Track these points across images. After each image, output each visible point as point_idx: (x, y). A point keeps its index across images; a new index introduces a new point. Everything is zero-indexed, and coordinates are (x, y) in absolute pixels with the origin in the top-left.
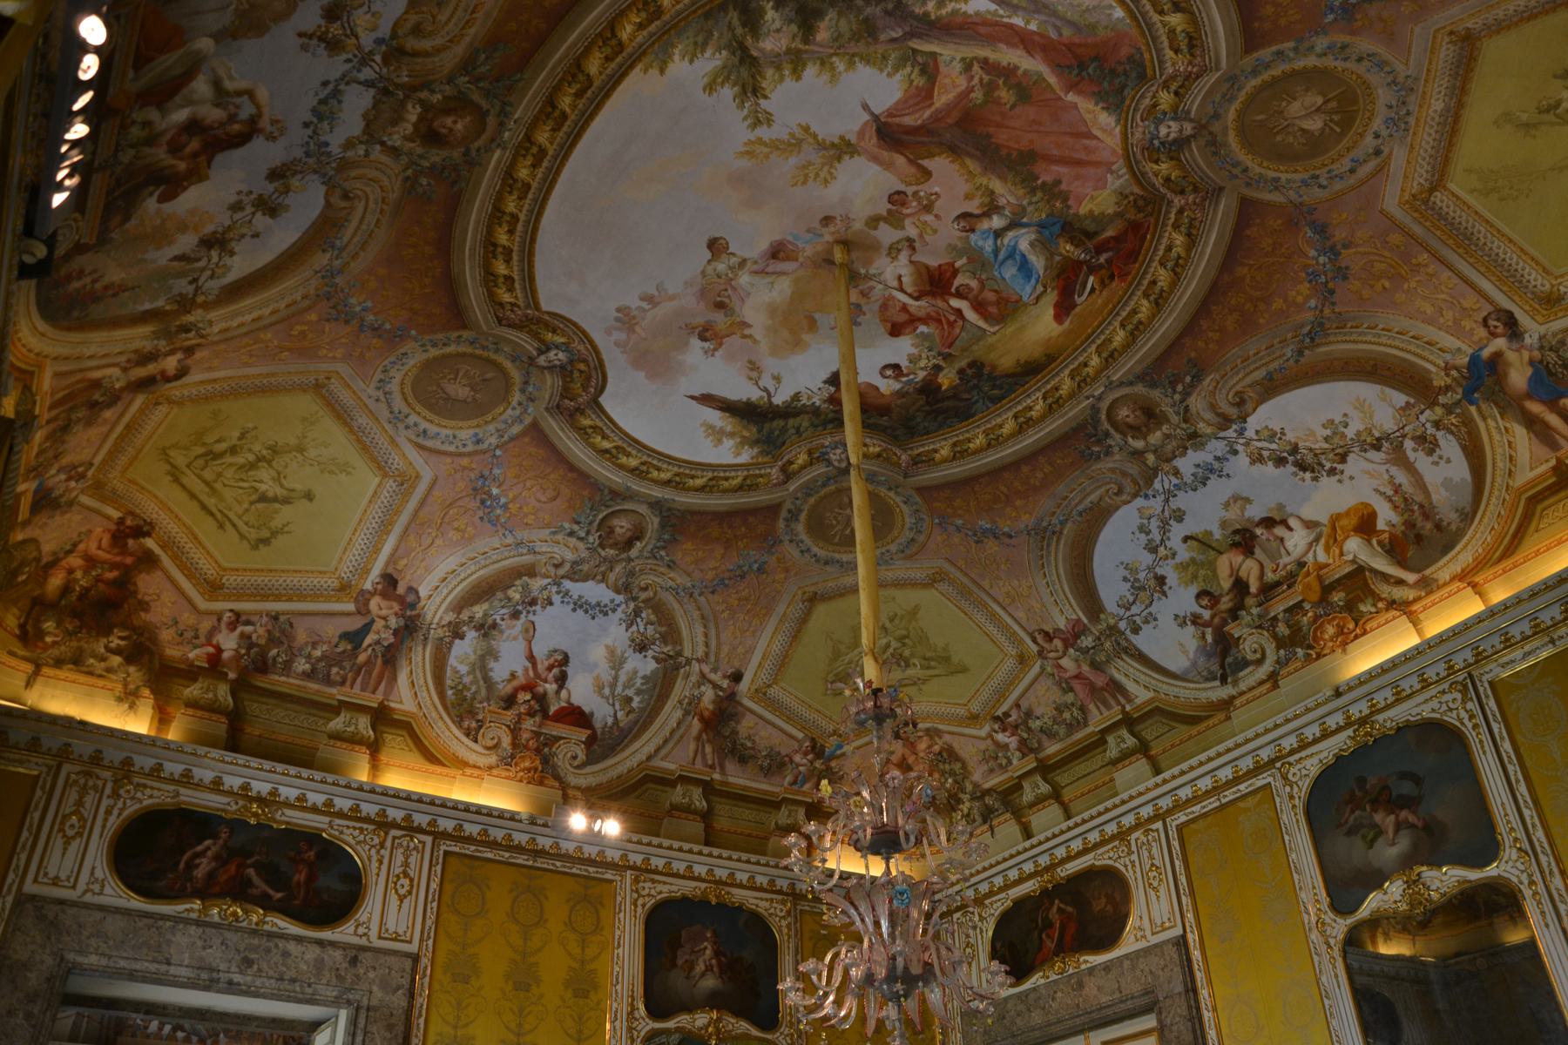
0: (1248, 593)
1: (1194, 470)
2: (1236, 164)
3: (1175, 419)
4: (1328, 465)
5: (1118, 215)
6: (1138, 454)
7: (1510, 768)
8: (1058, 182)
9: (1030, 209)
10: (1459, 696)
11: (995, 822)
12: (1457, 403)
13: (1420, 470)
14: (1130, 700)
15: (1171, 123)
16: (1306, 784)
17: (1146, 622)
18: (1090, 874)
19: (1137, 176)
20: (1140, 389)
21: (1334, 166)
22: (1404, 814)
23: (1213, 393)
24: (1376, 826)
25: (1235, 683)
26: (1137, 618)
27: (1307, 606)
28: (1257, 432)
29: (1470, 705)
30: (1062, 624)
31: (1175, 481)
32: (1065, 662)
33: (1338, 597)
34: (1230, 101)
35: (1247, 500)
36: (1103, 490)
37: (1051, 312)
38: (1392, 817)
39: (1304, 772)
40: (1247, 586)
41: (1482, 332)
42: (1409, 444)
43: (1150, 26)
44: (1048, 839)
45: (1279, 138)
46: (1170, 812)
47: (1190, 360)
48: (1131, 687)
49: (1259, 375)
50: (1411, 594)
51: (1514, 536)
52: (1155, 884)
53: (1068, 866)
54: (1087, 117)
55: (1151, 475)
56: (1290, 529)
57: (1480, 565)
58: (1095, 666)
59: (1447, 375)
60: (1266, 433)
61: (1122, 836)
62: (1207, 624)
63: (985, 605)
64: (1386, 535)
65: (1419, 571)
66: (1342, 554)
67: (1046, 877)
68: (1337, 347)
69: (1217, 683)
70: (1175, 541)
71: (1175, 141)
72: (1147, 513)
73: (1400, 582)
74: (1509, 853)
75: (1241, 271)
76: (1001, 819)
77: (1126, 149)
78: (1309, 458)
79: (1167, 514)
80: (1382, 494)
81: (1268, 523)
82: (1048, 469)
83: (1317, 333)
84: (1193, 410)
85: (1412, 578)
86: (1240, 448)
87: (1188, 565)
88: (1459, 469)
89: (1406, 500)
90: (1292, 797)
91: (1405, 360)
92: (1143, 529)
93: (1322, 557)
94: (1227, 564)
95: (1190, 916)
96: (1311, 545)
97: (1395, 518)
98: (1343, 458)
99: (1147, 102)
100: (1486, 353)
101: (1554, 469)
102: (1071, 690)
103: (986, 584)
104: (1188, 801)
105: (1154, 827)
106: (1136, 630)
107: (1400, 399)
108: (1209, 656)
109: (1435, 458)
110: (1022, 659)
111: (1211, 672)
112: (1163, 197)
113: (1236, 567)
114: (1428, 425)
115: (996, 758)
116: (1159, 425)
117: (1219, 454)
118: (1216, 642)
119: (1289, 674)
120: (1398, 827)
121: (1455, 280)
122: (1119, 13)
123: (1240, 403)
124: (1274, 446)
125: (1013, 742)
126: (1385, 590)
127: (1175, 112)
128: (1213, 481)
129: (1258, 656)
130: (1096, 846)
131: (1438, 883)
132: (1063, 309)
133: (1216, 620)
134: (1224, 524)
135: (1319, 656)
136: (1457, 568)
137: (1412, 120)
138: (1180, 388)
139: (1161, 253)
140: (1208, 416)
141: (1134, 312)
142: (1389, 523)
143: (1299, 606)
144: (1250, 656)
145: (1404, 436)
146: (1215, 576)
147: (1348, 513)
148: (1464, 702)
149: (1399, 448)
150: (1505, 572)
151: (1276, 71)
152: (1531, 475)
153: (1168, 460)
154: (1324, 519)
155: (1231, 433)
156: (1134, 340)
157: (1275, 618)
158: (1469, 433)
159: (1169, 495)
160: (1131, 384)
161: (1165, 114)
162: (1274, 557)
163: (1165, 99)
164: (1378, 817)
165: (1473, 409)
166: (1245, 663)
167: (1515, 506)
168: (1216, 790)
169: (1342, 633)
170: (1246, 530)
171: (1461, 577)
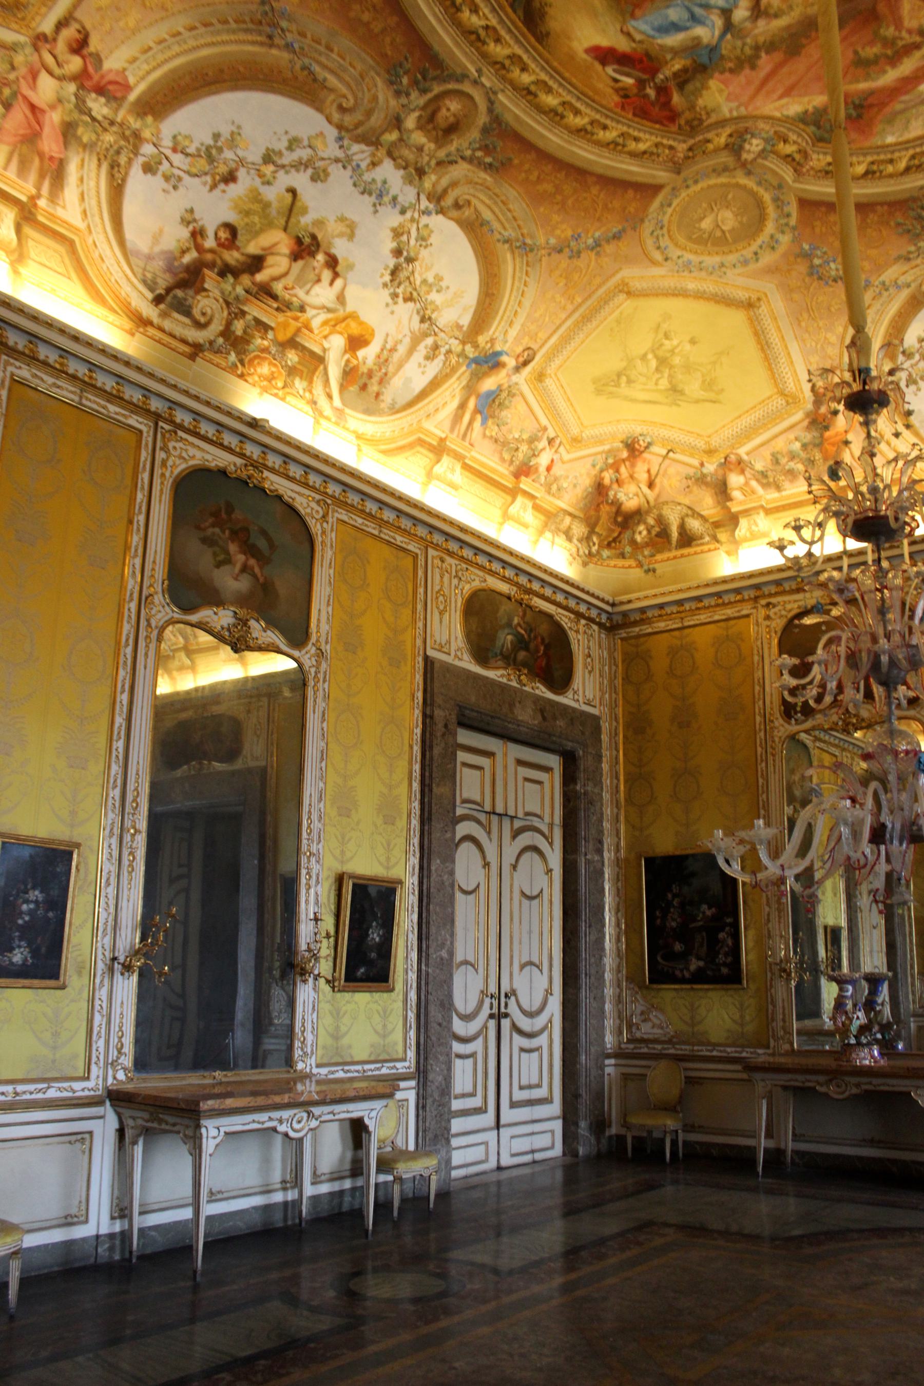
0: (252, 274)
2: (696, 182)
3: (441, 154)
4: (400, 291)
5: (692, 107)
6: (397, 122)
8: (753, 67)
9: (739, 43)
12: (466, 357)
15: (760, 148)
17: (167, 178)
19: (722, 123)
20: (483, 118)
21: (666, 237)
22: (252, 562)
23: (470, 182)
24: (227, 552)
26: (165, 165)
27: (270, 335)
28: (427, 226)
31: (363, 165)
33: (292, 357)
34: (759, 184)
35: (351, 236)
36: (344, 90)
37: (604, 42)
39: (184, 454)
41: (519, 349)
42: (430, 341)
43: (865, 155)
45: (704, 205)
47: (510, 160)
48: (70, 192)
49: (487, 215)
50: (328, 411)
54: (806, 99)
55: (371, 140)
56: (332, 283)
57: (371, 441)
58: (68, 131)
60: (425, 233)
62: (199, 248)
64: (355, 362)
68: (509, 265)
69: (150, 296)
70: (285, 180)
71: (741, 148)
72: (318, 143)
73: (330, 396)
74: (311, 648)
75: (595, 190)
77: (756, 118)
78: (402, 275)
79: (319, 164)
80: (386, 342)
81: (332, 262)
82: (377, 27)
83: (524, 248)
84: (452, 168)
85: (337, 402)
86: (408, 215)
87: (260, 201)
88: (420, 382)
89: (386, 360)
91: (497, 313)
92: (293, 143)
93: (316, 323)
94: (277, 241)
96: (323, 307)
97: (370, 362)
98: (409, 299)
99: (793, 137)
100: (504, 358)
101: (442, 440)
104: (45, 364)
106: (148, 169)
107: (466, 321)
108: (170, 269)
109: (423, 362)
111: (155, 283)
112: (693, 137)
113: (274, 250)
116: (436, 141)
117: (400, 199)
119: (210, 362)
120: (245, 569)
121: (558, 322)
122: (890, 140)
123: (457, 206)
124: (412, 242)
127: (772, 152)
128: (368, 200)
129: (202, 320)
132: (604, 55)
133: (209, 257)
134: (319, 223)
135: (241, 376)
137: (686, 273)
138: (479, 154)
139: (636, 134)
140: (444, 182)
141: (577, 112)
142: (365, 359)
143: (266, 328)
144: (196, 312)
146: (256, 234)
147: (361, 323)
149: (425, 335)
151: (771, 210)
153: (390, 154)
154: (350, 308)
155: (424, 203)
156: (545, 113)
157: (243, 313)
159: (345, 162)
160: (490, 111)
161: (773, 146)
162: (300, 281)
163: (789, 149)
164: (233, 548)
165: (464, 368)
166: (187, 312)
167: (412, 433)
169: (270, 381)
171: (359, 437)
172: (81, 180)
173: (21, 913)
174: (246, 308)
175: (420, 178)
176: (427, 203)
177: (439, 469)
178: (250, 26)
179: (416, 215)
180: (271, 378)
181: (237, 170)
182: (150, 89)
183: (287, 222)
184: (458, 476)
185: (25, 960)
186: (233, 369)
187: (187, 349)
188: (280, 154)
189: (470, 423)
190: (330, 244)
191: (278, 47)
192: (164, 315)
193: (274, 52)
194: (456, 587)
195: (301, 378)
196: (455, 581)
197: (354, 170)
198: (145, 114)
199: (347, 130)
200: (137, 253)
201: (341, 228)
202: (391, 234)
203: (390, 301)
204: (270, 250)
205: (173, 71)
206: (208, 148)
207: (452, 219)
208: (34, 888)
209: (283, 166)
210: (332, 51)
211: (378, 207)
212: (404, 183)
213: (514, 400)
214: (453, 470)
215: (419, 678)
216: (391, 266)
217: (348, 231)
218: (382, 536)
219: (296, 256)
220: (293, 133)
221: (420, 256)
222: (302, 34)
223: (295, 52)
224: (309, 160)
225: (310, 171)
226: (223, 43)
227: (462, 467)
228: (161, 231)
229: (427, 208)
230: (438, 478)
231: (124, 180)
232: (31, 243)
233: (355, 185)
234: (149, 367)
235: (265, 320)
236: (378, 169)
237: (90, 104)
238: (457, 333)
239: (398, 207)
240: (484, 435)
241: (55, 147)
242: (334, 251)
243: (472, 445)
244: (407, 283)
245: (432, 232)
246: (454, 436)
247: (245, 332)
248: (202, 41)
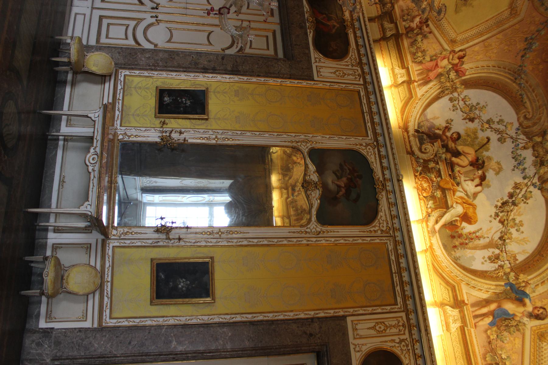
0: (453, 156)
1: (523, 156)
4: (501, 214)
7: (351, 239)
10: (384, 229)
11: (378, 6)
12: (508, 279)
13: (483, 251)
14: (419, 85)
16: (364, 152)
17: (454, 106)
18: (347, 43)
22: (343, 190)
24: (341, 178)
25: (414, 136)
26: (457, 102)
27: (439, 179)
28: (531, 192)
29: (379, 232)
30: (465, 66)
31: (521, 145)
32: (445, 62)
33: (438, 194)
35: (497, 173)
36: (530, 110)
38: (343, 185)
39: (370, 154)
40: (456, 157)
42: (497, 251)
44: (366, 29)
46: (366, 89)
48: (425, 88)
50: (431, 224)
51: (441, 274)
52: (337, 73)
53: (352, 35)
55: (529, 136)
56: (476, 186)
58: (440, 75)
59: (524, 281)
60: (528, 195)
61: (360, 64)
62: (444, 132)
63: (487, 32)
64: (459, 225)
65: (439, 231)
66: (457, 203)
67: (349, 24)
69: (416, 128)
72: (509, 127)
73: (437, 222)
74: (319, 228)
76: (379, 9)
78: (507, 208)
80: (478, 231)
81: (483, 178)
85: (437, 227)
86: (526, 181)
87: (475, 135)
88: (477, 266)
89: (472, 239)
90: (361, 145)
91: (539, 269)
92: (501, 121)
93: (458, 194)
94: (470, 153)
95: (321, 85)
96: (466, 192)
97: (465, 231)
98: (502, 222)
100: (527, 301)
101: (464, 301)
102: (431, 60)
103: (500, 36)
104: (369, 98)
105: (361, 79)
106: (451, 100)
107: (521, 258)
108: (430, 128)
109: (486, 259)
110: (453, 42)
111: (421, 127)
113: (467, 155)
114: (503, 263)
115: (408, 15)
117: (526, 171)
118: (435, 134)
119: (411, 161)
120: (339, 186)
124: (520, 196)
125: (414, 25)
126: (435, 214)
129: (423, 150)
130: (359, 51)
131: (313, 195)
133: (444, 137)
134: (489, 158)
135: (416, 176)
136: (436, 247)
143: (440, 175)
144: (424, 146)
145: (502, 251)
147: (475, 213)
148: (382, 231)
150: (428, 265)
152: (464, 292)
153: (533, 147)
154: (476, 202)
155: (535, 180)
157: (437, 163)
158: (492, 277)
159: (514, 140)
162: (466, 174)
164: (344, 179)
165: (503, 283)
166: (421, 142)
168: (371, 112)
169: (422, 190)
170: (483, 167)
171: (431, 247)
172: (431, 88)
173: (182, 99)
174: (440, 163)
175: (540, 166)
176: (537, 181)
177: (448, 308)
178: (512, 73)
179: (529, 183)
180: (424, 189)
181: (476, 119)
182: (470, 78)
183: (479, 149)
184: (455, 326)
185: (165, 101)
186: (415, 171)
187: (409, 150)
188: (494, 122)
189: (484, 315)
190: (488, 170)
191: (516, 83)
192: (414, 136)
193: (514, 84)
194: (393, 341)
195: (434, 203)
196: (397, 339)
197: (515, 146)
198: (463, 85)
199: (523, 128)
200: (425, 116)
201: (496, 166)
202: (514, 185)
203: (493, 216)
204: (465, 154)
205: (480, 77)
206: (473, 106)
207: (543, 195)
208: (191, 102)
209: (492, 128)
210: (534, 92)
211: (515, 169)
212: (532, 165)
213: (517, 332)
214: (455, 321)
215: (331, 313)
216: (505, 200)
217: (498, 170)
218: (394, 275)
219: (472, 164)
220: (503, 118)
221: (520, 205)
222: (527, 82)
223: (521, 88)
224: (502, 131)
225: (499, 136)
226: (500, 75)
227: (460, 327)
228: (438, 118)
229: (536, 183)
230: (445, 312)
231: (442, 97)
232: (402, 87)
233: (512, 152)
234: (393, 141)
235: (442, 173)
236: (525, 151)
237: (451, 73)
238: (512, 261)
239: (524, 174)
240: (486, 331)
241: (432, 76)
242: (487, 174)
243: (475, 326)
244: (506, 214)
245: (532, 197)
246: (471, 309)
247: (432, 168)
248: (494, 72)
